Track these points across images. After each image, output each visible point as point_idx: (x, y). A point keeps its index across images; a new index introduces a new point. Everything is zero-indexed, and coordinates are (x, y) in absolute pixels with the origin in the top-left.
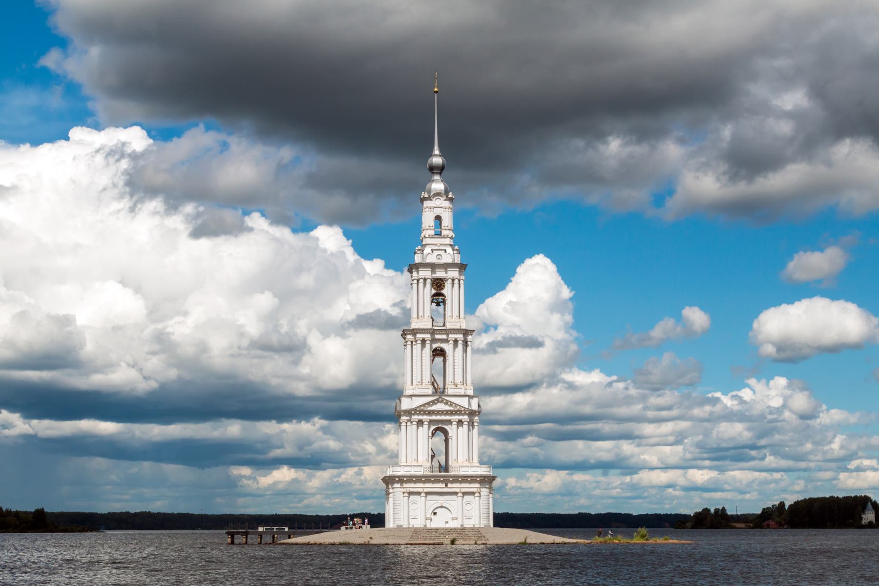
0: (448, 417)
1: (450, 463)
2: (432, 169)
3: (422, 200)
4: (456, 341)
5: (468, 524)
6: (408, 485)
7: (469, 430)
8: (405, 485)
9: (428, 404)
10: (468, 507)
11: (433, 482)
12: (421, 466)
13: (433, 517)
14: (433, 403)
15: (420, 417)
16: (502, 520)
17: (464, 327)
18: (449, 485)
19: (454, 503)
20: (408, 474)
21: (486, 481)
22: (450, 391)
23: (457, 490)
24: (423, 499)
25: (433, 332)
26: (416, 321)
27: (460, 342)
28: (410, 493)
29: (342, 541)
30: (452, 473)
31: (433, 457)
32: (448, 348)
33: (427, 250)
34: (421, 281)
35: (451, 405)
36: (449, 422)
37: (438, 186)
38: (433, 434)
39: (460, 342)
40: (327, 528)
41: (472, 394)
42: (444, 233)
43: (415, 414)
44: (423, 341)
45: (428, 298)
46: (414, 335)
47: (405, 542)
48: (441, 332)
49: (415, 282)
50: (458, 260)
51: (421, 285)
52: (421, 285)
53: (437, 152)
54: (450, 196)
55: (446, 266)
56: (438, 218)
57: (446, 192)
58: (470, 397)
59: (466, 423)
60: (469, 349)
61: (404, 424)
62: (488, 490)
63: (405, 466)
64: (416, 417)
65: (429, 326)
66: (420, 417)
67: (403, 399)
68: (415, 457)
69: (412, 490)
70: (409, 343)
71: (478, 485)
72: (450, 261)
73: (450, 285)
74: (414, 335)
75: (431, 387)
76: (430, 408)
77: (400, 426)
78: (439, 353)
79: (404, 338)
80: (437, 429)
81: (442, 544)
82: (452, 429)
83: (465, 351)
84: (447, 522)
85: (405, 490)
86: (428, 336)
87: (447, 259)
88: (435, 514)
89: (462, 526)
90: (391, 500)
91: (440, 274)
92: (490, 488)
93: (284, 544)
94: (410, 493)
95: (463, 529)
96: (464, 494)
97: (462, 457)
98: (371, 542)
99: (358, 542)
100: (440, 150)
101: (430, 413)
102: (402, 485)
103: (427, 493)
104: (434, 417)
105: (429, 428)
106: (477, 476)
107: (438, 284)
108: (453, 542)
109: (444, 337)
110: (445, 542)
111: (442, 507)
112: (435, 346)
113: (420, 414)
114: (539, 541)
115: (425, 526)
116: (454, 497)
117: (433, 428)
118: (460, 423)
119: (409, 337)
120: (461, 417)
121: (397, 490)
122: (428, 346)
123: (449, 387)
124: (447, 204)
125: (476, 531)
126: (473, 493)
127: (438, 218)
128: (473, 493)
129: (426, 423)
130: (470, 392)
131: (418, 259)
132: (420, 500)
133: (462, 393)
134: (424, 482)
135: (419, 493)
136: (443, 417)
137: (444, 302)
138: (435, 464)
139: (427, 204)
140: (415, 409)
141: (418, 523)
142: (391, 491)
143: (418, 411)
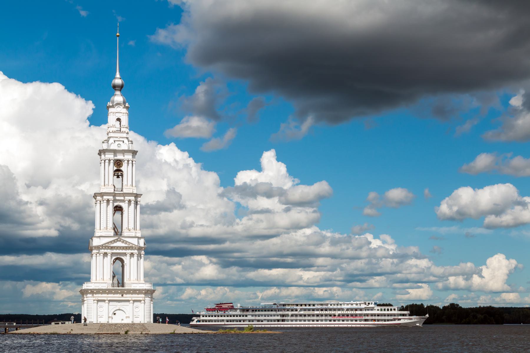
0: (124, 251)
1: (125, 281)
2: (115, 87)
3: (108, 108)
4: (130, 201)
5: (137, 321)
6: (97, 295)
7: (138, 260)
8: (95, 295)
9: (111, 242)
10: (137, 310)
11: (114, 294)
12: (106, 283)
13: (113, 316)
14: (114, 241)
15: (106, 251)
16: (159, 318)
17: (135, 192)
18: (124, 295)
19: (128, 307)
20: (97, 288)
21: (149, 293)
22: (125, 233)
23: (130, 299)
24: (107, 304)
25: (114, 195)
26: (104, 187)
27: (133, 202)
28: (98, 301)
29: (52, 332)
30: (127, 287)
31: (114, 277)
32: (124, 205)
33: (111, 141)
34: (107, 161)
35: (126, 243)
36: (125, 254)
37: (118, 98)
38: (114, 262)
39: (133, 202)
40: (42, 323)
41: (140, 236)
42: (122, 129)
43: (102, 248)
44: (108, 201)
45: (111, 173)
46: (102, 196)
47: (95, 332)
48: (120, 195)
49: (103, 161)
51: (107, 164)
52: (107, 164)
53: (118, 75)
54: (127, 105)
55: (124, 152)
56: (119, 120)
57: (124, 103)
58: (139, 238)
59: (136, 255)
60: (138, 207)
61: (94, 255)
62: (150, 299)
63: (95, 283)
64: (103, 251)
65: (112, 191)
66: (106, 251)
67: (94, 239)
68: (102, 277)
69: (99, 299)
70: (98, 202)
71: (143, 296)
72: (126, 148)
73: (126, 164)
74: (102, 196)
75: (113, 231)
76: (112, 245)
77: (92, 256)
78: (118, 209)
79: (95, 199)
80: (116, 259)
81: (119, 334)
82: (126, 259)
83: (136, 208)
84: (122, 320)
85: (95, 299)
86: (111, 198)
87: (124, 147)
88: (115, 314)
89: (132, 322)
90: (85, 305)
91: (120, 157)
92: (152, 298)
93: (13, 334)
94: (98, 301)
95: (133, 324)
96: (134, 301)
97: (134, 277)
98: (72, 333)
99: (63, 333)
100: (120, 75)
101: (112, 248)
102: (93, 295)
103: (110, 301)
104: (115, 251)
105: (111, 258)
106: (143, 290)
107: (118, 163)
108: (126, 333)
109: (122, 198)
110: (121, 333)
111: (119, 310)
112: (116, 204)
113: (105, 249)
114: (182, 332)
115: (108, 322)
116: (127, 303)
117: (114, 258)
118: (132, 255)
119: (99, 198)
120: (132, 251)
121: (89, 299)
122: (111, 204)
123: (125, 231)
124: (125, 110)
125: (142, 326)
126: (140, 301)
128: (140, 301)
129: (109, 255)
130: (139, 235)
132: (105, 305)
133: (134, 235)
134: (108, 294)
135: (104, 301)
136: (121, 251)
137: (122, 175)
138: (116, 281)
139: (111, 110)
140: (102, 246)
141: (104, 320)
142: (85, 299)
143: (103, 247)
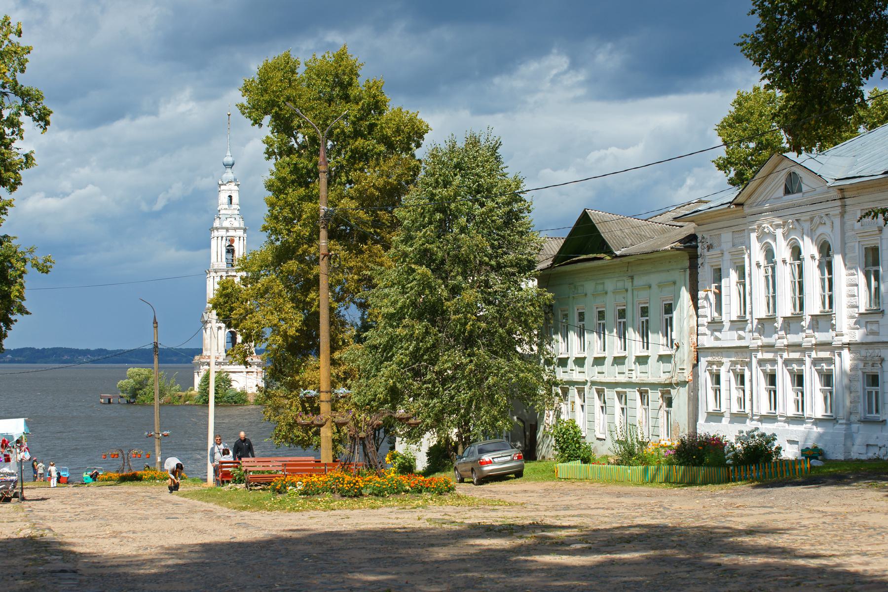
50: (242, 226)
53: (229, 154)
55: (235, 229)
56: (230, 197)
72: (238, 226)
87: (236, 224)
91: (231, 233)
124: (236, 188)
127: (230, 197)
131: (217, 224)
139: (223, 187)
